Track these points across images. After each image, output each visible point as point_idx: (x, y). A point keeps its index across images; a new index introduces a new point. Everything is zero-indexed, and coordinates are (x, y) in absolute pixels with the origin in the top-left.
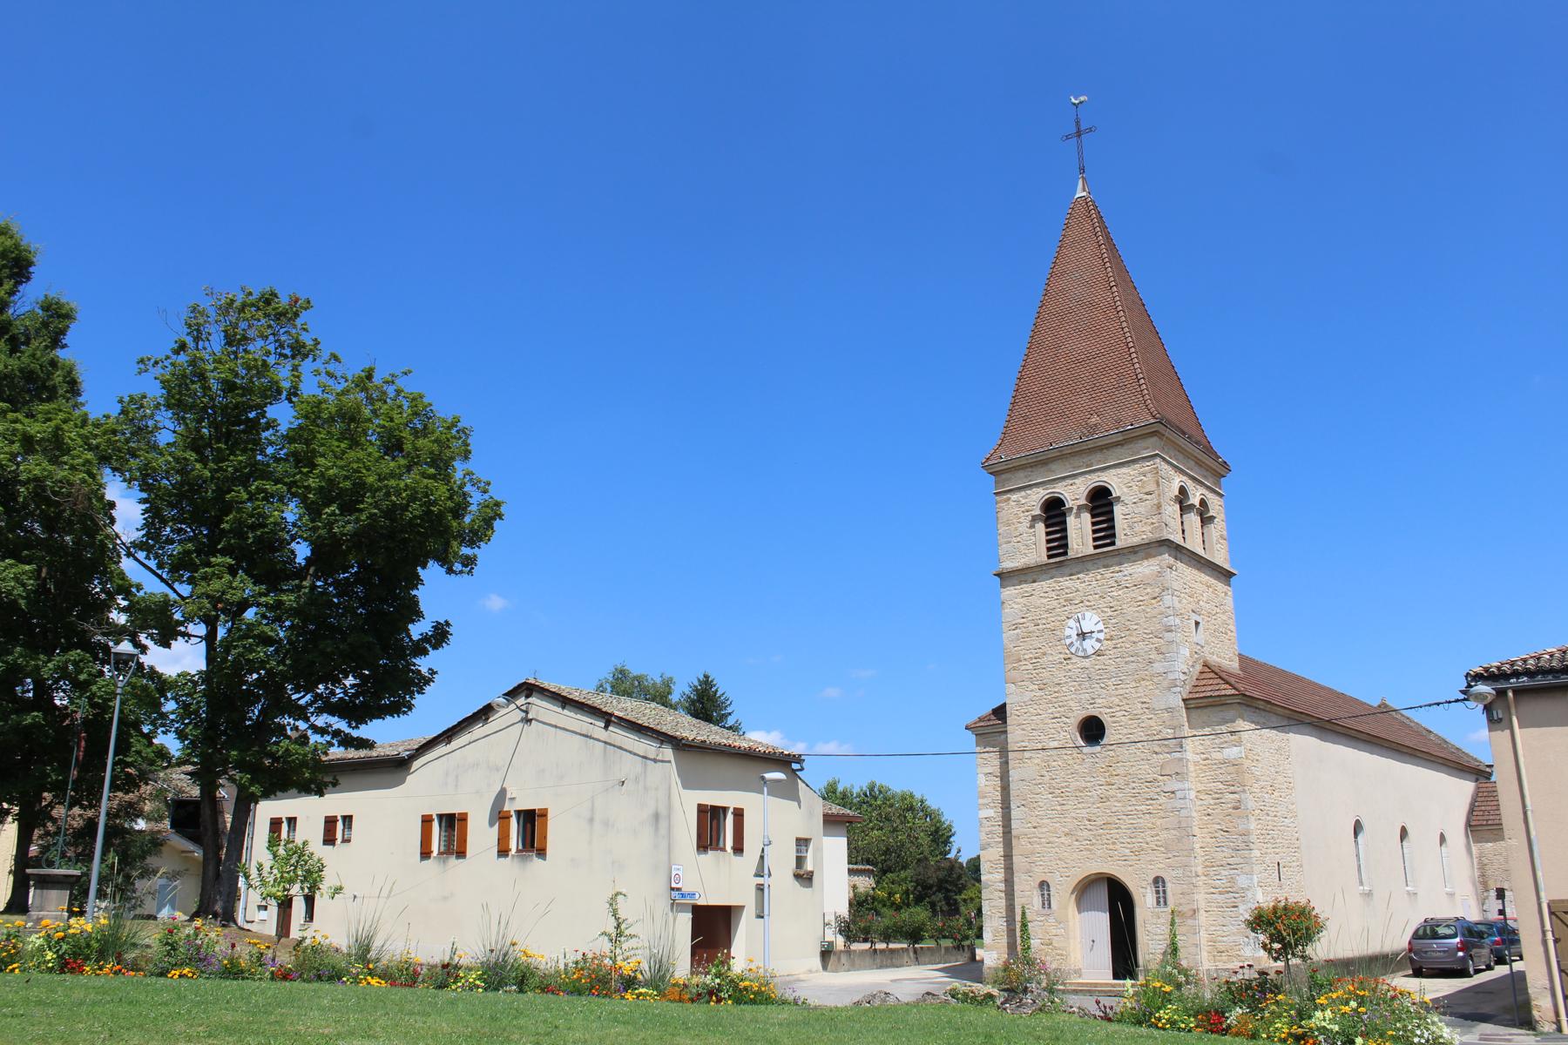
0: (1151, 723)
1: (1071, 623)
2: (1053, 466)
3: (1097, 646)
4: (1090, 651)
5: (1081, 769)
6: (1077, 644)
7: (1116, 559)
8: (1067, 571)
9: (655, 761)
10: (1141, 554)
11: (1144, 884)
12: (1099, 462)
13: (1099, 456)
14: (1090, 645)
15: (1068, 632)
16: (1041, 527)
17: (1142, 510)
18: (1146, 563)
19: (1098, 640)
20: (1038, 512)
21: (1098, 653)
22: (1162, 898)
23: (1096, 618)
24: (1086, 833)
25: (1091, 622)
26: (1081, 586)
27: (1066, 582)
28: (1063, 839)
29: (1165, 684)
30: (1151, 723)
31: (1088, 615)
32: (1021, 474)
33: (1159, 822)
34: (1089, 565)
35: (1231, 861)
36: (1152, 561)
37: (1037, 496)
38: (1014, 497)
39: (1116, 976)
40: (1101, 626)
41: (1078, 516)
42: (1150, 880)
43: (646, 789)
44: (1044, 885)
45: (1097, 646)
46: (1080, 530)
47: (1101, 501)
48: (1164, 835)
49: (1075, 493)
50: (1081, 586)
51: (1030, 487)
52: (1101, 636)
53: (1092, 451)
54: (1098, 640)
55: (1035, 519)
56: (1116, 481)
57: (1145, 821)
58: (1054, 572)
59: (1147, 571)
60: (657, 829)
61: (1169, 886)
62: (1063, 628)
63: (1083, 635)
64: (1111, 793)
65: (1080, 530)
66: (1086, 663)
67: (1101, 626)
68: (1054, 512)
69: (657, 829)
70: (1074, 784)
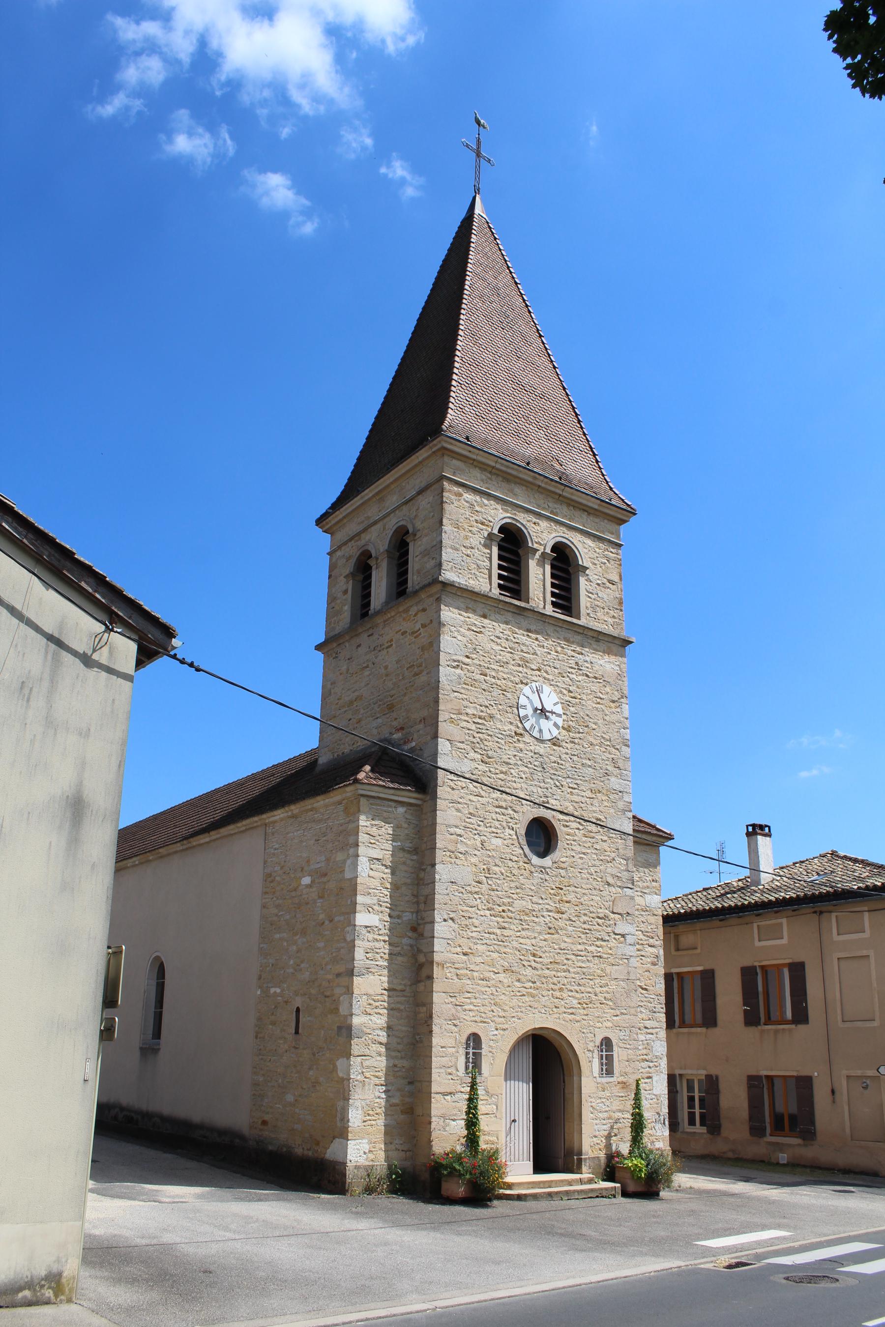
0: (605, 846)
1: (527, 690)
2: (518, 490)
3: (555, 732)
4: (546, 736)
5: (528, 884)
6: (533, 720)
7: (578, 638)
8: (525, 623)
9: (87, 660)
10: (603, 646)
11: (591, 1046)
12: (565, 517)
13: (565, 509)
14: (548, 729)
15: (523, 701)
16: (495, 550)
17: (605, 597)
18: (606, 657)
19: (555, 725)
20: (496, 531)
21: (555, 742)
22: (608, 1068)
23: (554, 698)
24: (529, 972)
25: (550, 700)
26: (539, 650)
27: (522, 636)
28: (501, 976)
29: (621, 805)
30: (605, 846)
31: (547, 689)
32: (477, 473)
33: (609, 969)
34: (550, 629)
35: (648, 1024)
36: (613, 658)
37: (497, 516)
38: (468, 496)
39: (539, 1167)
40: (558, 709)
41: (541, 563)
42: (598, 1043)
43: (50, 723)
44: (475, 1040)
45: (555, 732)
46: (539, 578)
47: (564, 563)
48: (613, 986)
49: (542, 535)
50: (539, 650)
51: (489, 496)
52: (560, 722)
53: (561, 499)
54: (555, 725)
55: (490, 535)
56: (586, 550)
57: (594, 967)
58: (509, 616)
59: (608, 667)
60: (74, 842)
61: (618, 1053)
62: (517, 694)
63: (543, 712)
64: (561, 923)
65: (539, 578)
66: (541, 749)
67: (558, 709)
68: (511, 544)
69: (74, 842)
70: (519, 904)
